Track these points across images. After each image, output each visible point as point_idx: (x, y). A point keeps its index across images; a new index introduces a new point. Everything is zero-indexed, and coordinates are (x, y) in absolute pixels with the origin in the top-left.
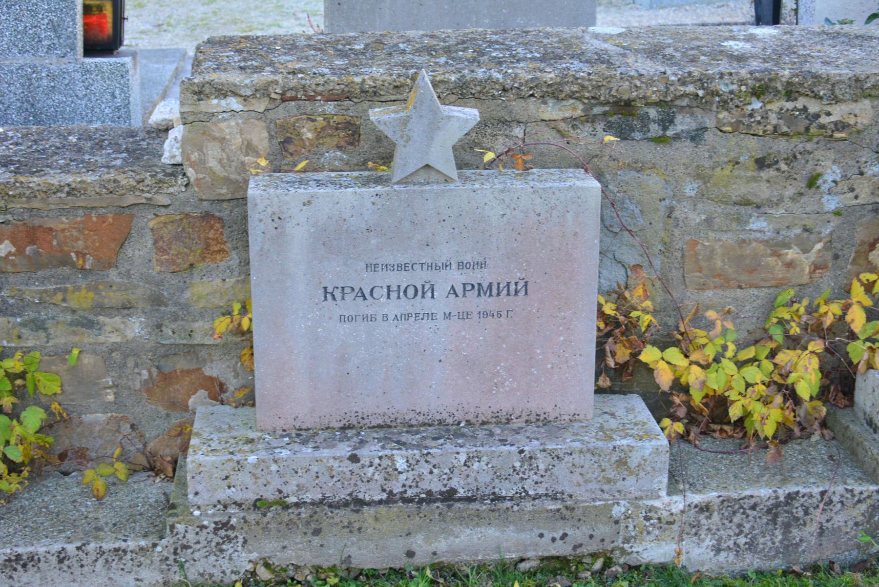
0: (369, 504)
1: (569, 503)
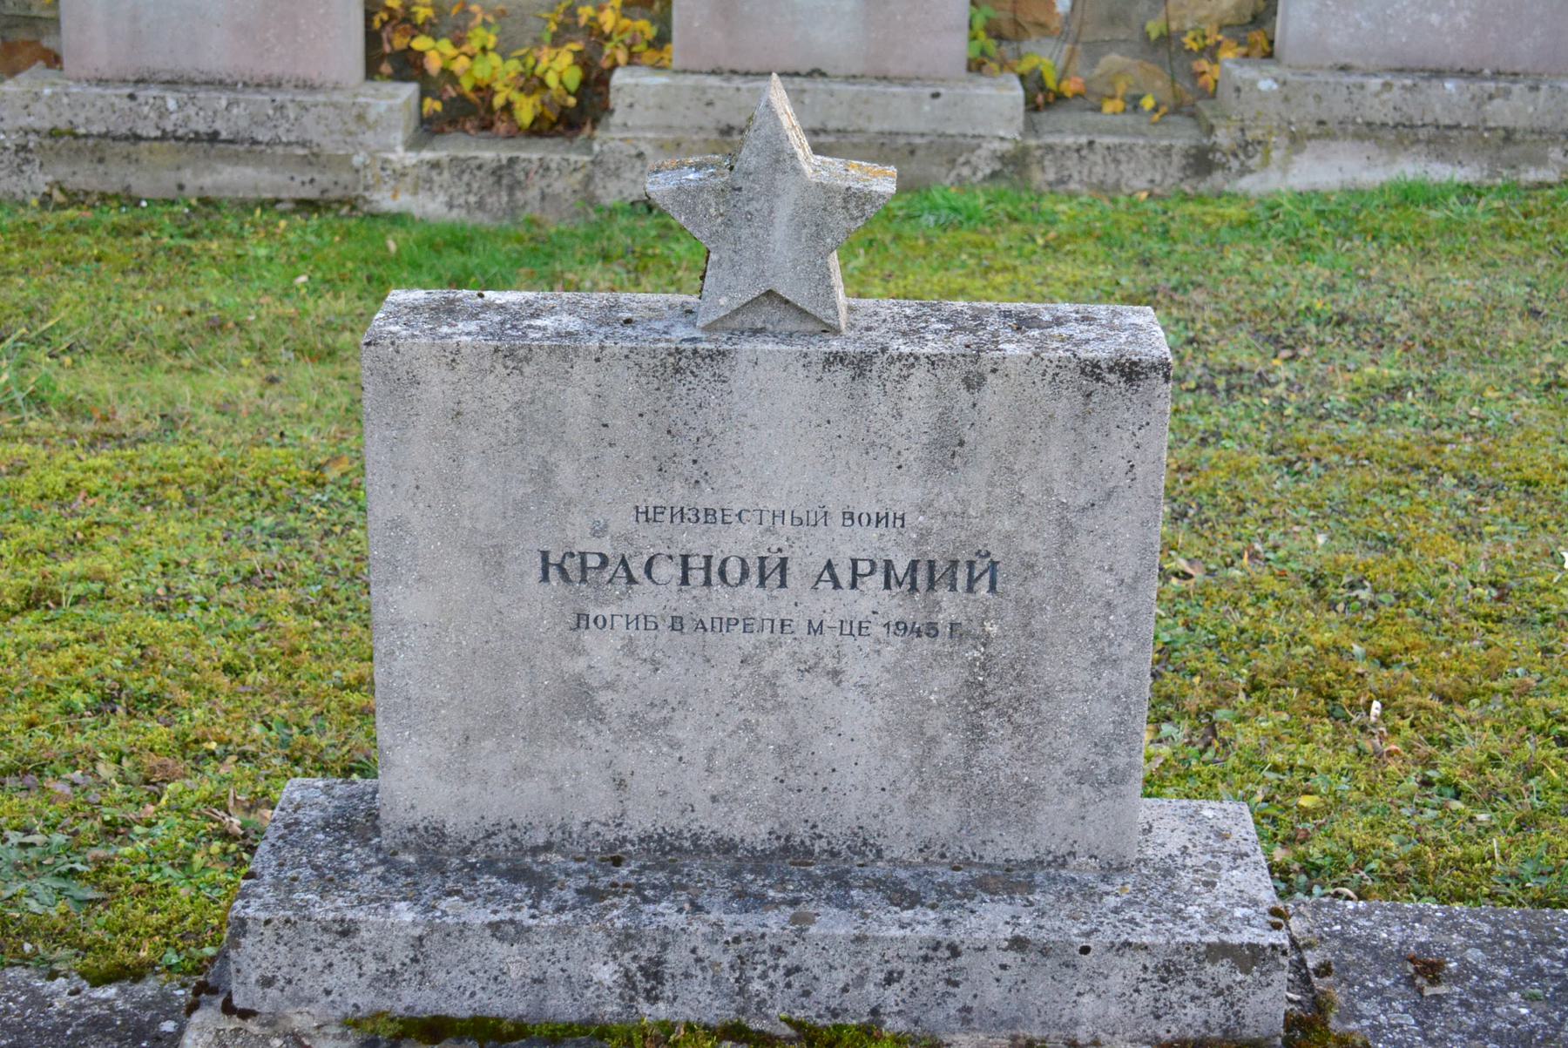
0: (147, 139)
1: (316, 150)
